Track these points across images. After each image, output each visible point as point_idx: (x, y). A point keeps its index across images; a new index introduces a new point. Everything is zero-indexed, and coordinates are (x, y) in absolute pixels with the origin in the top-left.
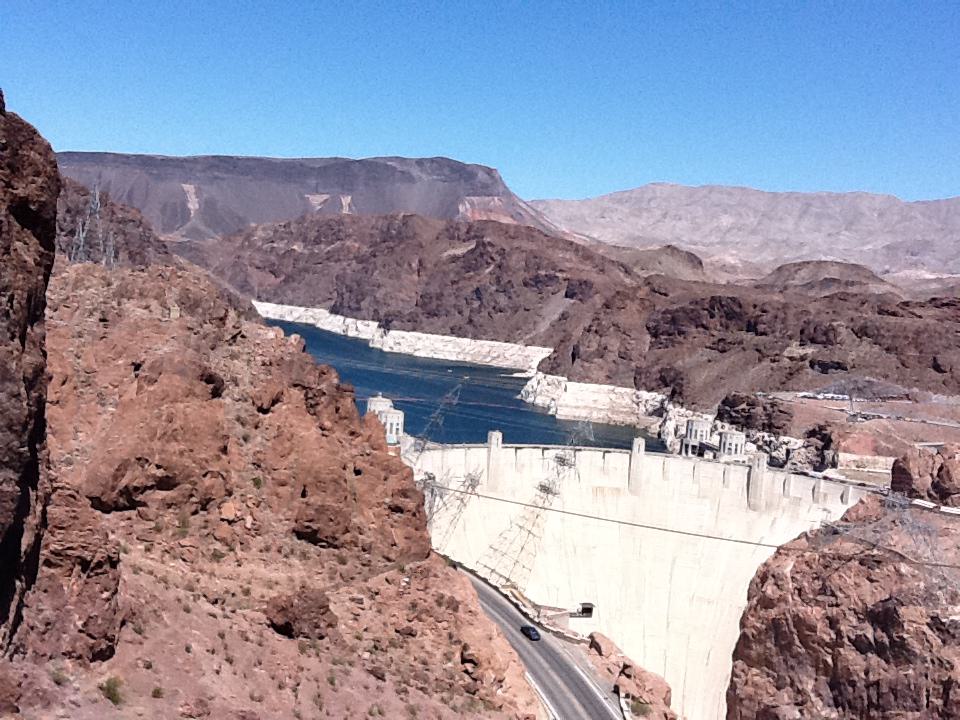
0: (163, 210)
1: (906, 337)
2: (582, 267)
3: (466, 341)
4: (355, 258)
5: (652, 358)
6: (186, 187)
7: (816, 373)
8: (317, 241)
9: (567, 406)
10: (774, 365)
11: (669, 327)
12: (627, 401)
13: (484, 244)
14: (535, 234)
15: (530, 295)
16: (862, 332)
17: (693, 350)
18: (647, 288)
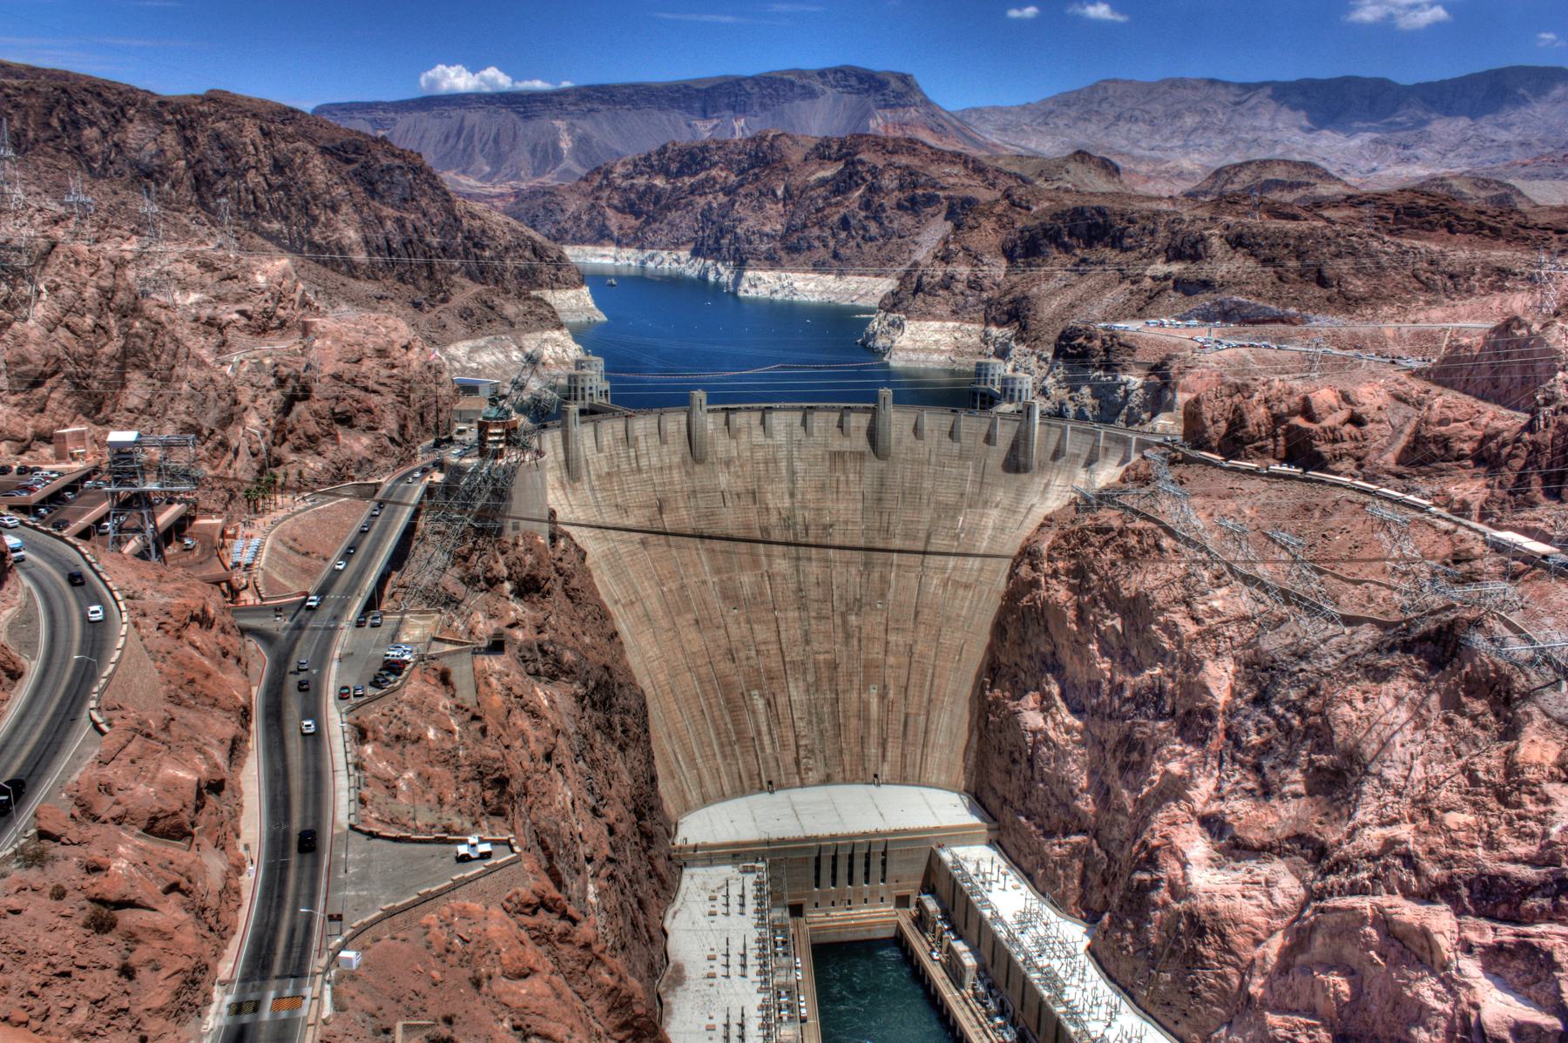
0: (533, 152)
1: (1287, 246)
2: (966, 181)
3: (831, 277)
4: (722, 189)
5: (1005, 286)
6: (558, 123)
7: (1179, 295)
8: (680, 173)
9: (902, 349)
10: (1134, 288)
11: (1026, 249)
12: (975, 339)
13: (853, 163)
14: (919, 146)
15: (908, 220)
16: (1237, 242)
17: (1048, 277)
18: (1005, 203)
